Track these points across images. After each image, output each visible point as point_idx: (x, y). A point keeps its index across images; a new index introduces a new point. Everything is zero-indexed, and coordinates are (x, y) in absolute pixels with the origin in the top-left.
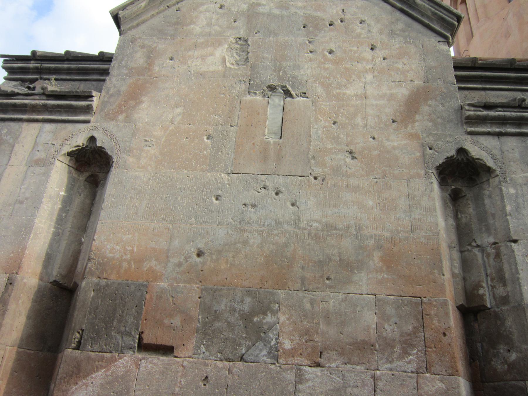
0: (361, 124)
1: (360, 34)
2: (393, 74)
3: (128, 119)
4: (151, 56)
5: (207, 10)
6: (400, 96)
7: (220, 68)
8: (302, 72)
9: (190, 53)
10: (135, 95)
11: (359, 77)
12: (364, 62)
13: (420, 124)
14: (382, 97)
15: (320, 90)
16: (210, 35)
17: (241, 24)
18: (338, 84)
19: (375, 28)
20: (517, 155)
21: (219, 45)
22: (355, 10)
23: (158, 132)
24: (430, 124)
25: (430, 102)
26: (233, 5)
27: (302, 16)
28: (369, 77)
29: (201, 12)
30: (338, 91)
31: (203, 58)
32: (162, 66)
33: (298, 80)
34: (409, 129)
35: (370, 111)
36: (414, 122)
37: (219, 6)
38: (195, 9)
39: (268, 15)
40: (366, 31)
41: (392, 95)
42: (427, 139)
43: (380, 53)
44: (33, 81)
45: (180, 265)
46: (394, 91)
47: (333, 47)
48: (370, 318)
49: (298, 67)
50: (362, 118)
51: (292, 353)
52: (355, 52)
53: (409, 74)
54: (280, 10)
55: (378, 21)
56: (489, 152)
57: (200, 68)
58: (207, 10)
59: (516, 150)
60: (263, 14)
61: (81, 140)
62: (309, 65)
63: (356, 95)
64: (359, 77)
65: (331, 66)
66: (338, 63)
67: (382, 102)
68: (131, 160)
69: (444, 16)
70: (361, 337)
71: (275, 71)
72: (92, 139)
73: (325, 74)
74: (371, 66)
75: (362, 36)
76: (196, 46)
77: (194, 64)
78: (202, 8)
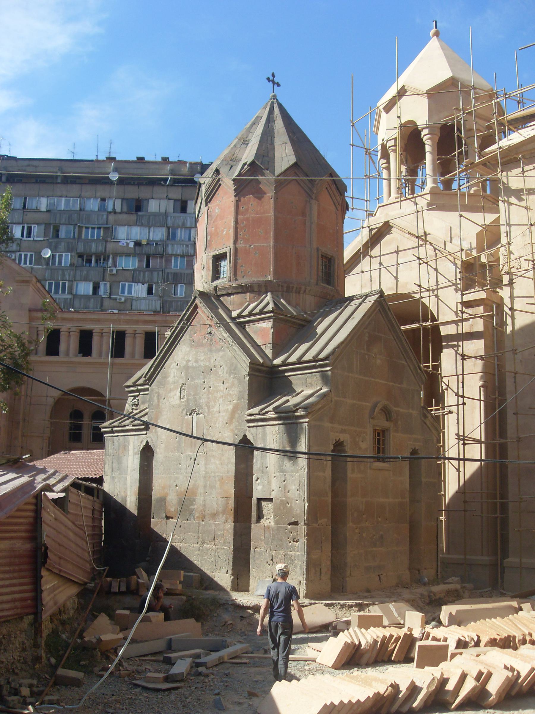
4: (159, 396)
6: (230, 410)
7: (177, 402)
13: (235, 423)
15: (206, 410)
19: (226, 369)
22: (219, 359)
23: (164, 437)
31: (173, 396)
35: (221, 419)
41: (228, 409)
43: (226, 385)
44: (137, 396)
45: (172, 490)
48: (215, 506)
49: (200, 398)
51: (198, 517)
55: (226, 366)
61: (144, 443)
67: (224, 414)
68: (158, 450)
70: (213, 512)
72: (147, 442)
76: (171, 390)
78: (172, 367)
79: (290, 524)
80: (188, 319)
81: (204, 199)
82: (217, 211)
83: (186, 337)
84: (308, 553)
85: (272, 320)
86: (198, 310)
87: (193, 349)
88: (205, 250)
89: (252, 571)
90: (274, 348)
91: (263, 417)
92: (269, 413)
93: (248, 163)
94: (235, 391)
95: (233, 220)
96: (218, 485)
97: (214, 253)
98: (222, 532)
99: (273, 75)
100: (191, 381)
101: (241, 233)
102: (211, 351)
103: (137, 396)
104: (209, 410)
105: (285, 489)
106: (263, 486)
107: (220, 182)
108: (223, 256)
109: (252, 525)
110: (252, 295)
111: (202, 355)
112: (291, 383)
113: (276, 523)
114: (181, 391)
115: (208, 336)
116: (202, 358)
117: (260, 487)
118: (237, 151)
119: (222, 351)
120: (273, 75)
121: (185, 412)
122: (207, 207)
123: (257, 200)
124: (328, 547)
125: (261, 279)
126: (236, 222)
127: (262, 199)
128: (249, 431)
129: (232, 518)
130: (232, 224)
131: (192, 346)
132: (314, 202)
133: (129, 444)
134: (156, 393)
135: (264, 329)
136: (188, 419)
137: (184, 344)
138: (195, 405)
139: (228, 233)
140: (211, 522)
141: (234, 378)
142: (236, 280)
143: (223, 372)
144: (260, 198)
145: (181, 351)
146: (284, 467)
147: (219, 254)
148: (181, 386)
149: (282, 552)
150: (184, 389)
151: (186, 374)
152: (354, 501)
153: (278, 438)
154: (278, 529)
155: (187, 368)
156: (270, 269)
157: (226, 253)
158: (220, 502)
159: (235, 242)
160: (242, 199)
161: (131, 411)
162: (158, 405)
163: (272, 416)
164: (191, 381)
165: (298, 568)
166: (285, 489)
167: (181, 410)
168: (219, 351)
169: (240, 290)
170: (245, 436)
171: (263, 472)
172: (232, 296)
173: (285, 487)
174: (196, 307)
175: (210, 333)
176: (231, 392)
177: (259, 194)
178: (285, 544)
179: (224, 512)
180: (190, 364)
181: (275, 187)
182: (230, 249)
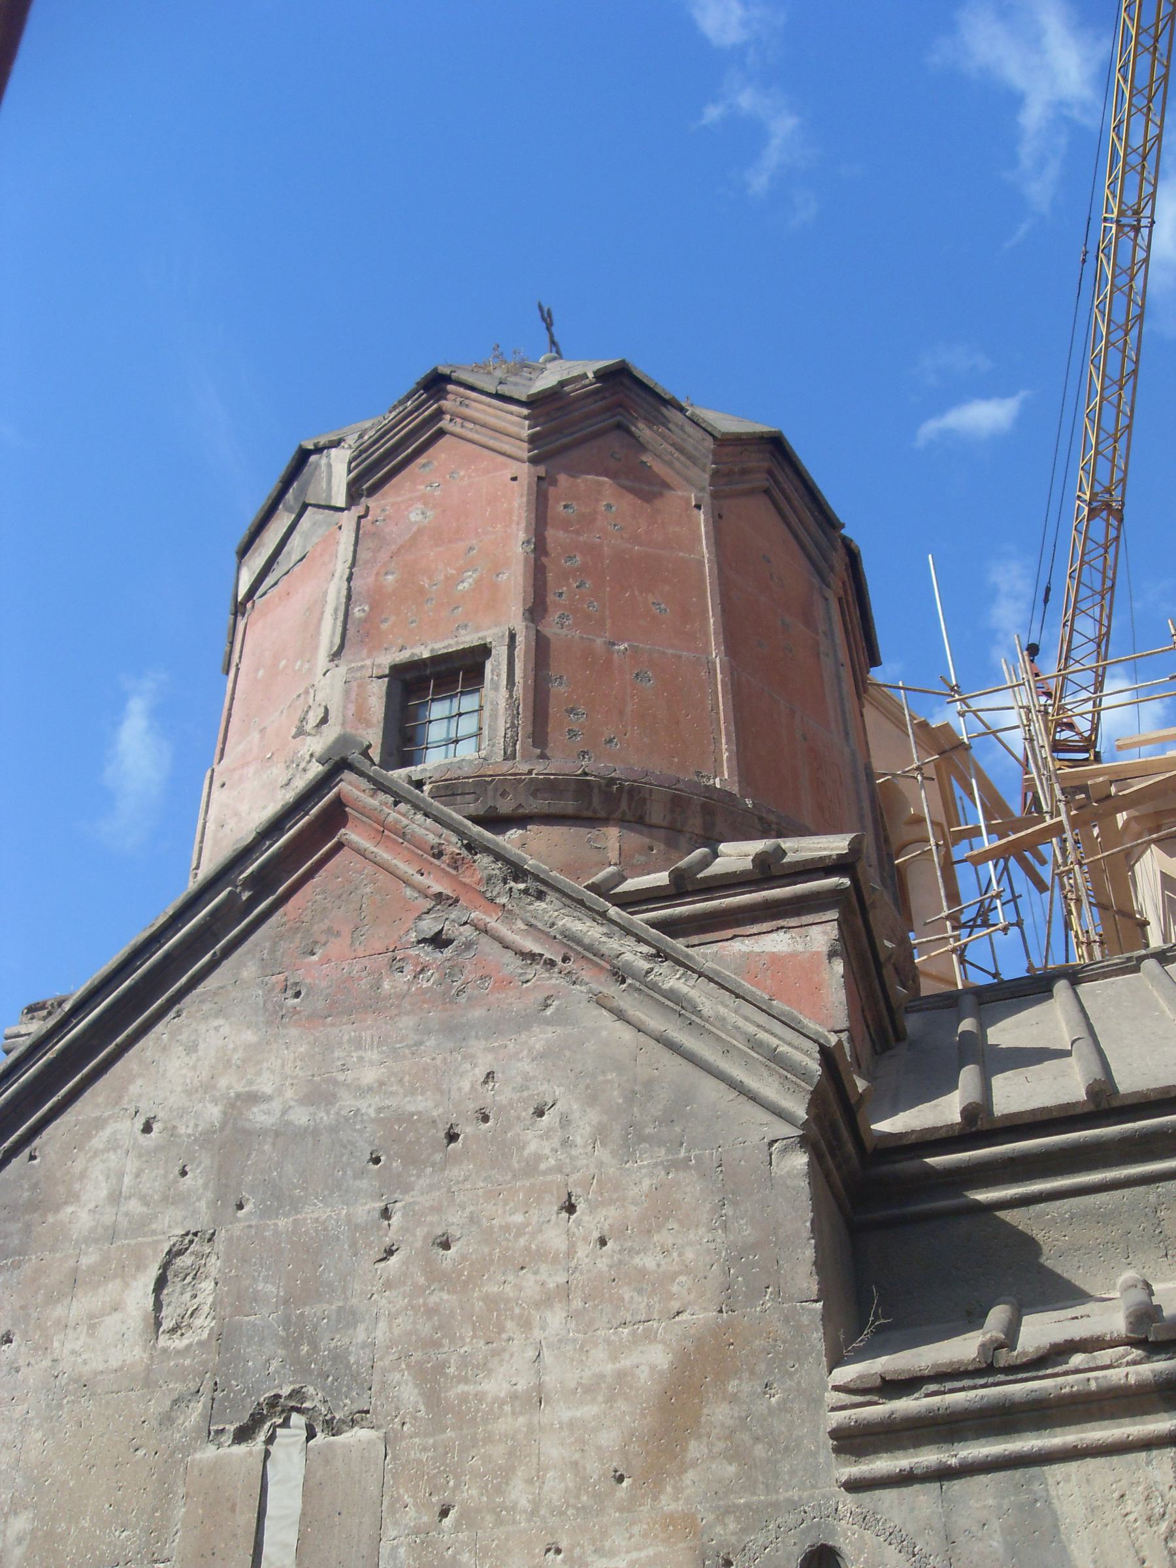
0: (524, 1502)
1: (538, 1158)
2: (627, 1293)
5: (113, 1145)
6: (643, 1374)
7: (134, 1354)
8: (361, 1334)
9: (59, 1311)
11: (526, 1324)
12: (544, 1268)
14: (589, 1389)
15: (409, 1393)
16: (112, 1234)
17: (200, 1182)
18: (464, 1361)
19: (585, 1123)
20: (996, 1544)
21: (138, 1268)
22: (526, 1066)
24: (732, 1469)
25: (732, 1386)
26: (182, 1112)
27: (372, 1121)
28: (555, 1319)
29: (96, 1154)
30: (461, 1388)
31: (92, 1323)
33: (348, 1366)
34: (668, 1504)
35: (554, 1451)
36: (682, 1470)
37: (139, 1123)
38: (80, 1146)
39: (277, 1134)
40: (556, 1142)
41: (621, 1375)
42: (719, 1529)
46: (626, 1363)
47: (454, 1222)
49: (348, 1318)
50: (530, 1481)
52: (520, 1230)
53: (675, 1288)
54: (312, 1109)
55: (592, 1100)
57: (85, 1363)
58: (113, 1145)
59: (995, 1524)
60: (263, 1133)
63: (514, 1397)
64: (526, 1324)
65: (445, 1296)
66: (466, 1284)
67: (588, 1411)
69: (784, 1048)
71: (284, 1343)
73: (425, 1329)
74: (561, 1278)
75: (543, 1166)
76: (75, 1280)
77: (69, 1346)
78: (99, 1141)
80: (263, 883)
83: (243, 971)
85: (834, 914)
86: (350, 834)
87: (294, 1032)
88: (336, 655)
91: (1018, 1390)
92: (1077, 1360)
94: (686, 1253)
95: (522, 536)
97: (403, 656)
100: (266, 1212)
101: (560, 594)
102: (454, 1031)
104: (433, 1398)
107: (445, 423)
108: (460, 671)
110: (635, 839)
111: (373, 1055)
112: (1029, 1246)
114: (161, 1283)
115: (427, 954)
116: (369, 1076)
119: (548, 1022)
121: (195, 1412)
123: (630, 497)
126: (539, 547)
127: (658, 503)
128: (865, 1520)
130: (517, 548)
131: (277, 1017)
136: (216, 1466)
137: (220, 1012)
138: (300, 1367)
141: (671, 1166)
142: (543, 756)
144: (648, 497)
145: (191, 1048)
147: (436, 660)
148: (173, 1254)
155: (232, 1140)
156: (717, 753)
157: (484, 651)
159: (536, 610)
160: (563, 479)
163: (1116, 1376)
164: (266, 1212)
167: (157, 1405)
168: (523, 1023)
169: (568, 805)
174: (337, 815)
175: (438, 941)
176: (648, 1261)
177: (646, 487)
180: (260, 1117)
182: (512, 637)
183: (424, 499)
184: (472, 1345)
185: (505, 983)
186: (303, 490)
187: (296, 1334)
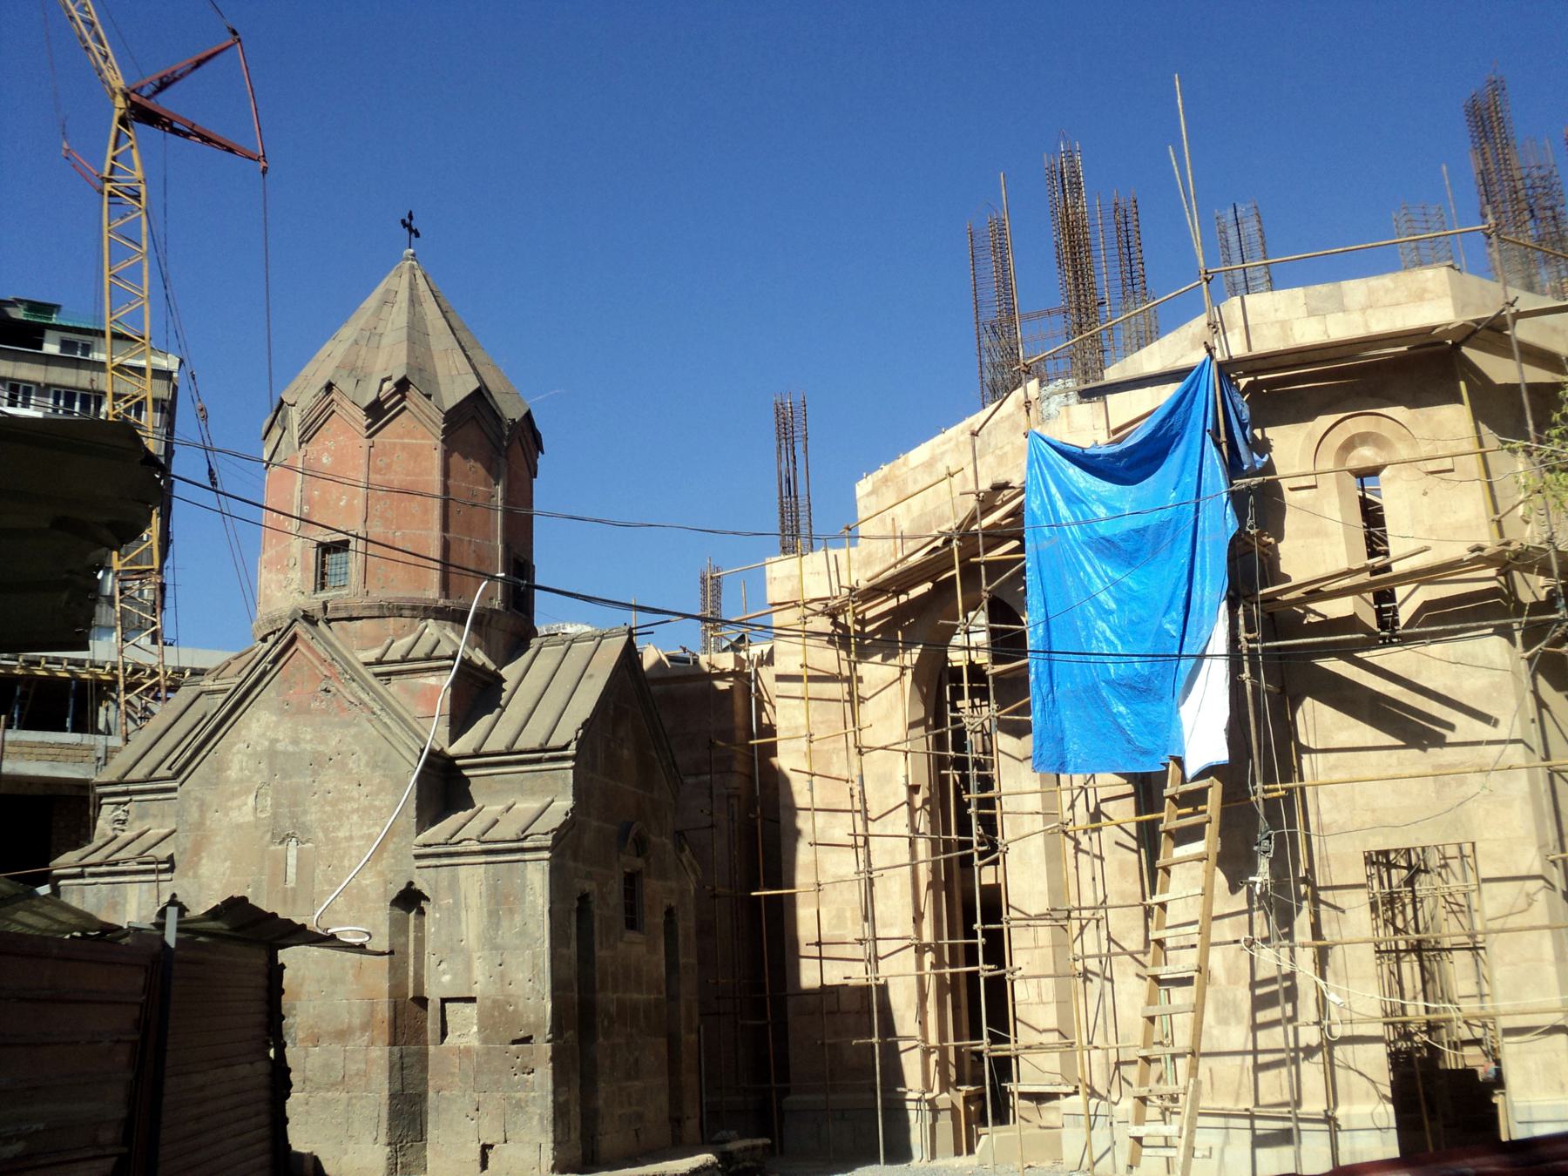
3: (196, 876)
4: (203, 807)
10: (197, 849)
13: (387, 860)
14: (362, 837)
15: (321, 835)
16: (242, 781)
19: (364, 759)
23: (216, 886)
28: (355, 817)
31: (240, 808)
32: (213, 819)
43: (365, 790)
44: (125, 803)
47: (330, 786)
49: (305, 812)
51: (302, 1040)
55: (366, 751)
56: (427, 881)
62: (314, 809)
76: (233, 796)
78: (235, 749)
79: (514, 1042)
80: (275, 661)
81: (295, 431)
82: (324, 460)
83: (269, 694)
84: (555, 1092)
86: (298, 644)
89: (432, 1133)
90: (452, 723)
91: (452, 849)
93: (395, 379)
96: (350, 977)
98: (363, 1066)
99: (411, 217)
100: (283, 778)
103: (125, 803)
105: (503, 979)
106: (455, 976)
109: (431, 1048)
113: (485, 1041)
117: (446, 978)
118: (363, 352)
120: (411, 217)
121: (269, 836)
122: (302, 452)
124: (576, 1079)
125: (418, 594)
129: (386, 1037)
131: (282, 712)
132: (502, 461)
133: (125, 899)
134: (196, 799)
135: (432, 687)
138: (295, 827)
139: (349, 504)
140: (336, 1047)
143: (358, 764)
146: (499, 940)
149: (499, 1095)
150: (266, 795)
151: (271, 764)
152: (608, 998)
153: (484, 889)
154: (488, 1053)
155: (272, 754)
158: (355, 1009)
161: (111, 834)
162: (200, 824)
165: (535, 1121)
166: (503, 979)
170: (411, 883)
171: (452, 950)
172: (359, 623)
173: (502, 976)
174: (294, 638)
178: (504, 1080)
179: (365, 1027)
180: (280, 747)
181: (444, 431)
183: (327, 450)
184: (336, 823)
185: (344, 710)
186: (284, 418)
187: (293, 816)
